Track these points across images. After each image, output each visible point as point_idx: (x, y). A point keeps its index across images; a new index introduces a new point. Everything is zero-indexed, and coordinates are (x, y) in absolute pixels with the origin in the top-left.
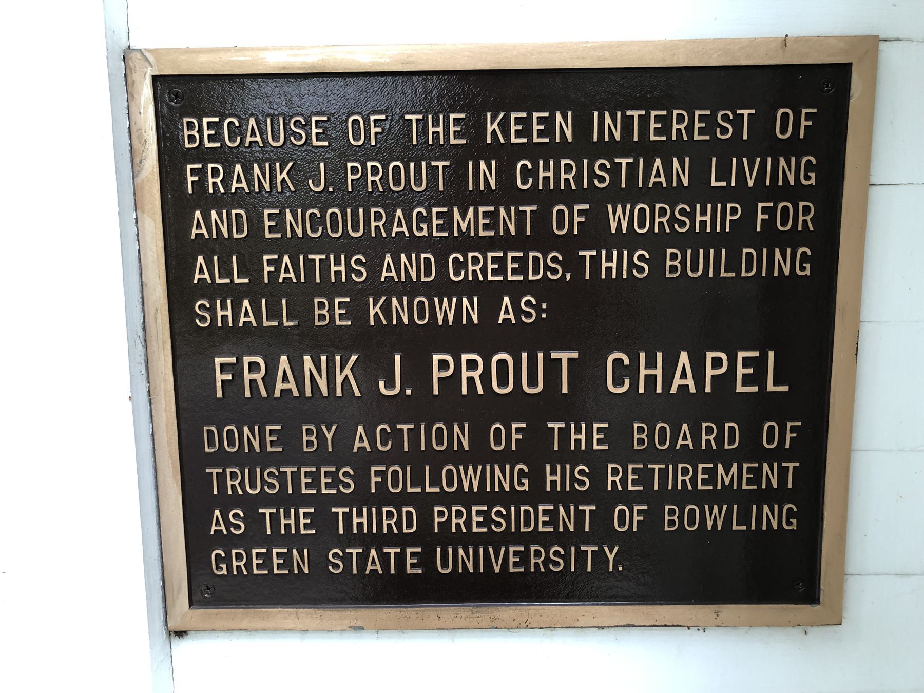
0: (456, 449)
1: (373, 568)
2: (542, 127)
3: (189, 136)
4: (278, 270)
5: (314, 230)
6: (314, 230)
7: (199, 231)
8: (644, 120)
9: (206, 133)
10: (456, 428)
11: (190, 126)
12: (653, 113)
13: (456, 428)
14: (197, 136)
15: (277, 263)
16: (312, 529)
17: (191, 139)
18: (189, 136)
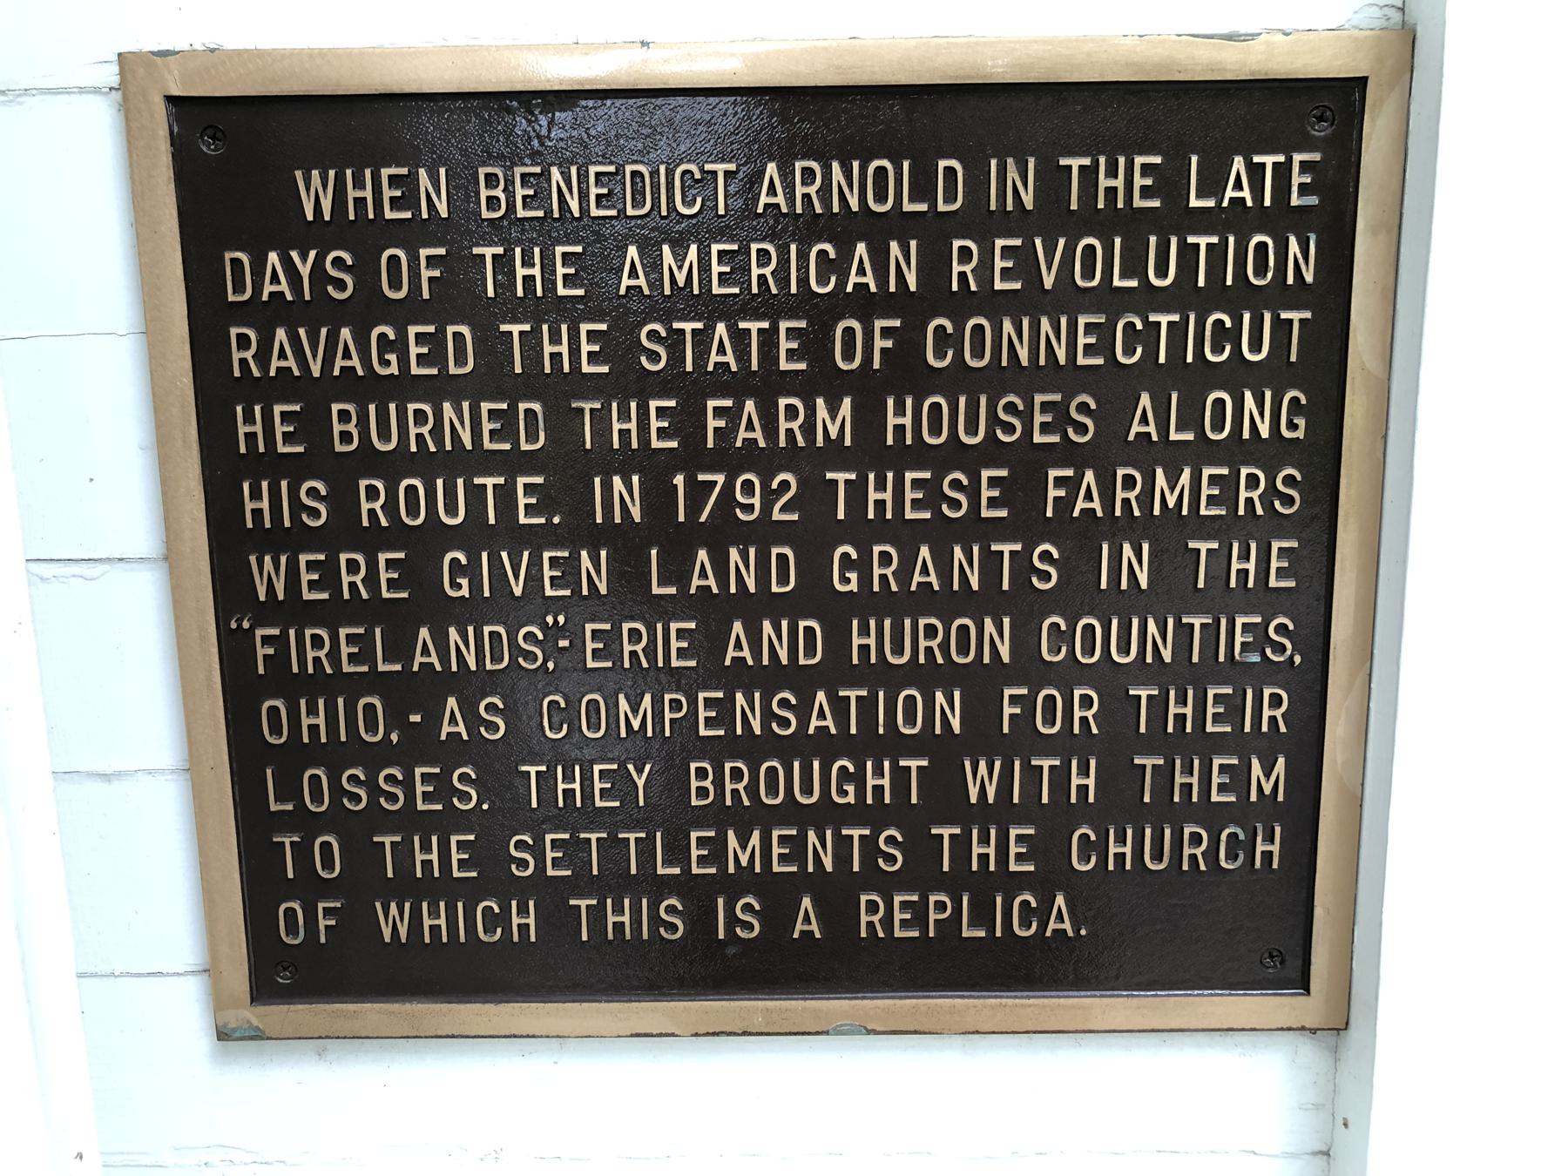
0: (938, 731)
1: (806, 928)
2: (1149, 182)
3: (489, 198)
4: (733, 428)
5: (1217, 350)
6: (1217, 350)
7: (721, 359)
8: (1282, 171)
9: (520, 192)
10: (940, 697)
11: (491, 180)
12: (1297, 158)
13: (940, 697)
14: (502, 197)
15: (732, 415)
16: (711, 865)
17: (493, 202)
18: (489, 198)
